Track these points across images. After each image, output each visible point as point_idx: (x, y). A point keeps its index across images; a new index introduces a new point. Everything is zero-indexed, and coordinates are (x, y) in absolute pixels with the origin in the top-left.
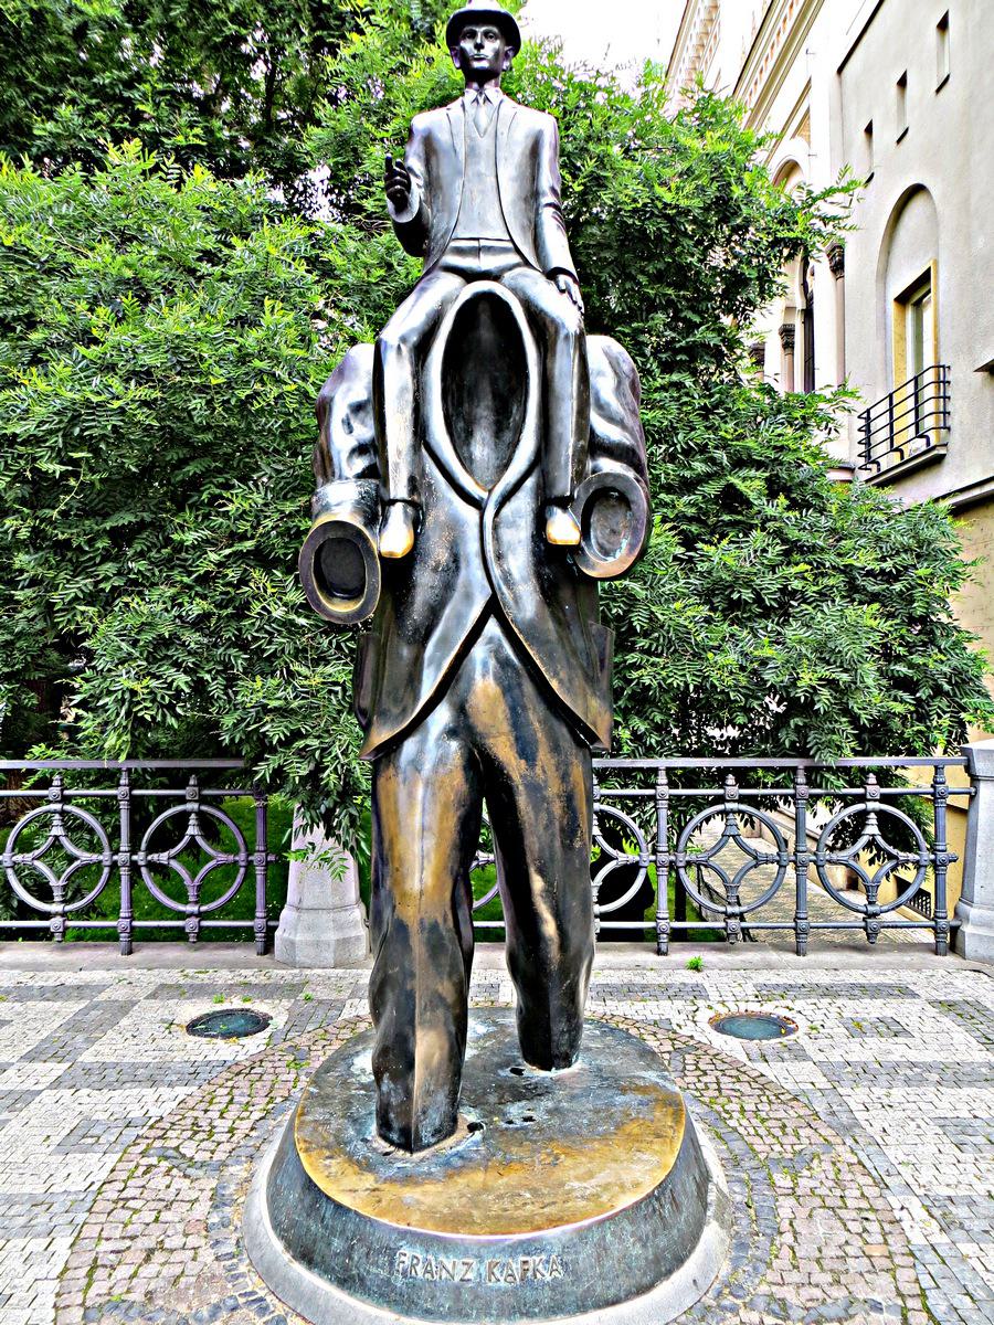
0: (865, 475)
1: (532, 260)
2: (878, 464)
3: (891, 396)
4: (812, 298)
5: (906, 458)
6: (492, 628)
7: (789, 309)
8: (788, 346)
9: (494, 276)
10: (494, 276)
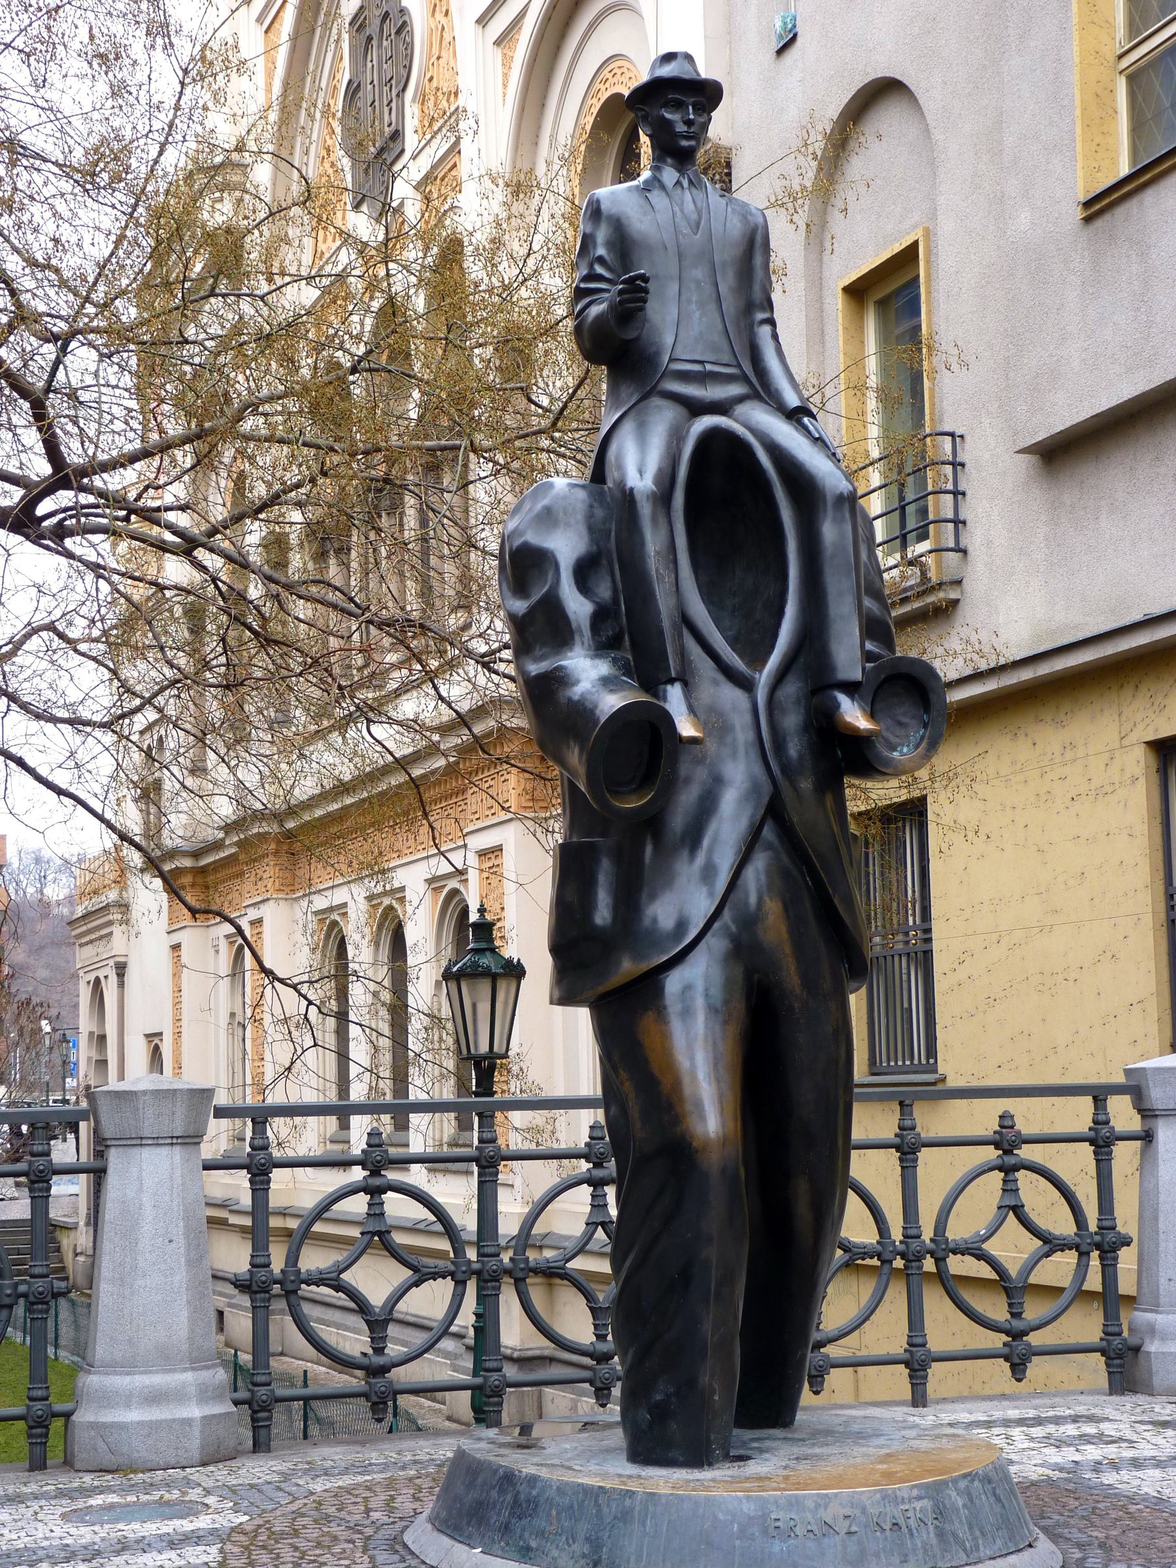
6: (768, 833)
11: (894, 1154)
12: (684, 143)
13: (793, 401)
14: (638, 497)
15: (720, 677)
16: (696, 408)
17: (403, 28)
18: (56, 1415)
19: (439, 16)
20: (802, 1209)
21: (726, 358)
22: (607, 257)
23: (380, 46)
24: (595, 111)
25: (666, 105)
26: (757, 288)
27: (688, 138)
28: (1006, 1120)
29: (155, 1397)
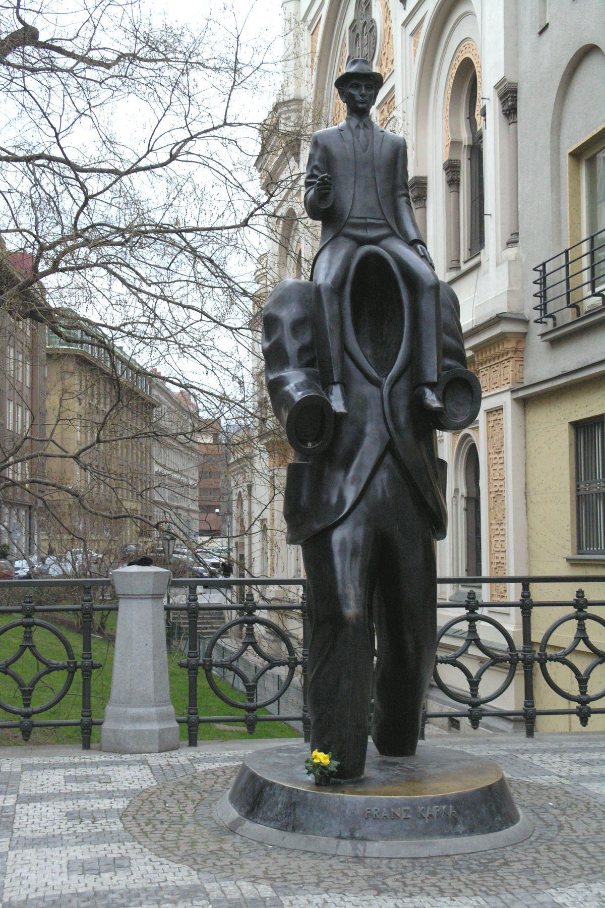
0: (540, 329)
1: (396, 229)
2: (554, 318)
3: (567, 252)
4: (481, 137)
5: (582, 315)
6: (388, 460)
7: (455, 144)
8: (453, 182)
9: (375, 241)
10: (375, 241)
11: (519, 610)
12: (360, 106)
13: (413, 235)
14: (322, 290)
15: (365, 380)
16: (361, 242)
17: (373, 29)
18: (94, 724)
19: (388, 22)
20: (410, 648)
21: (378, 215)
22: (319, 166)
23: (362, 38)
24: (457, 66)
25: (351, 86)
26: (399, 177)
27: (362, 103)
28: (580, 593)
29: (139, 719)
